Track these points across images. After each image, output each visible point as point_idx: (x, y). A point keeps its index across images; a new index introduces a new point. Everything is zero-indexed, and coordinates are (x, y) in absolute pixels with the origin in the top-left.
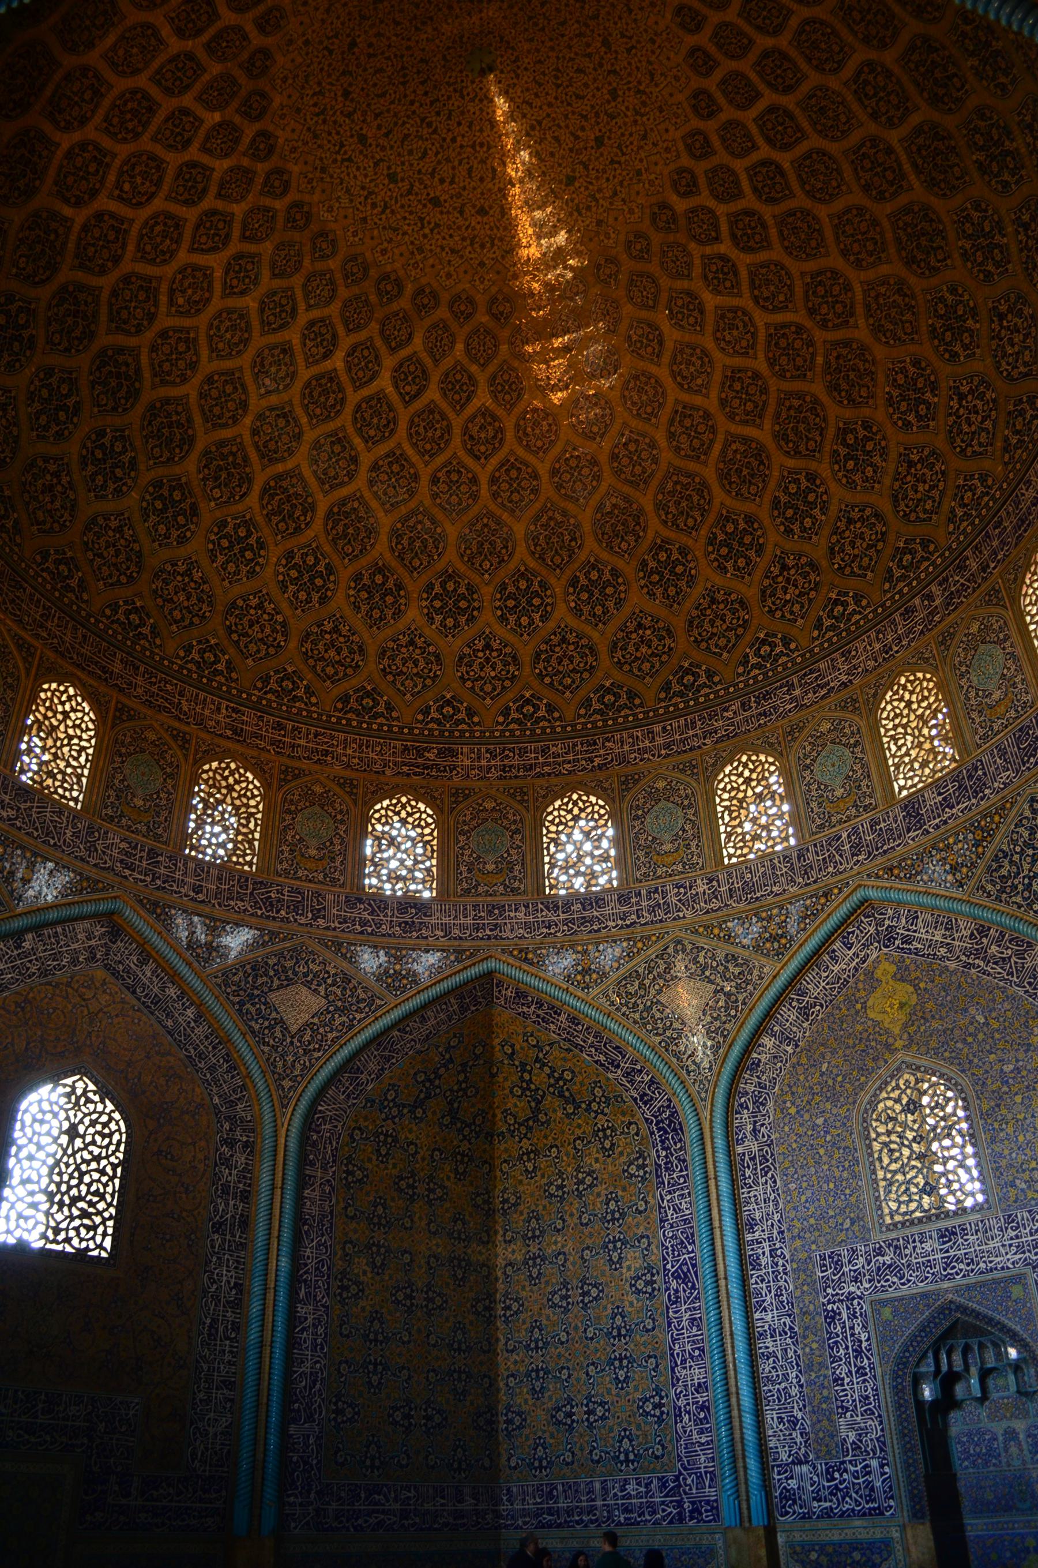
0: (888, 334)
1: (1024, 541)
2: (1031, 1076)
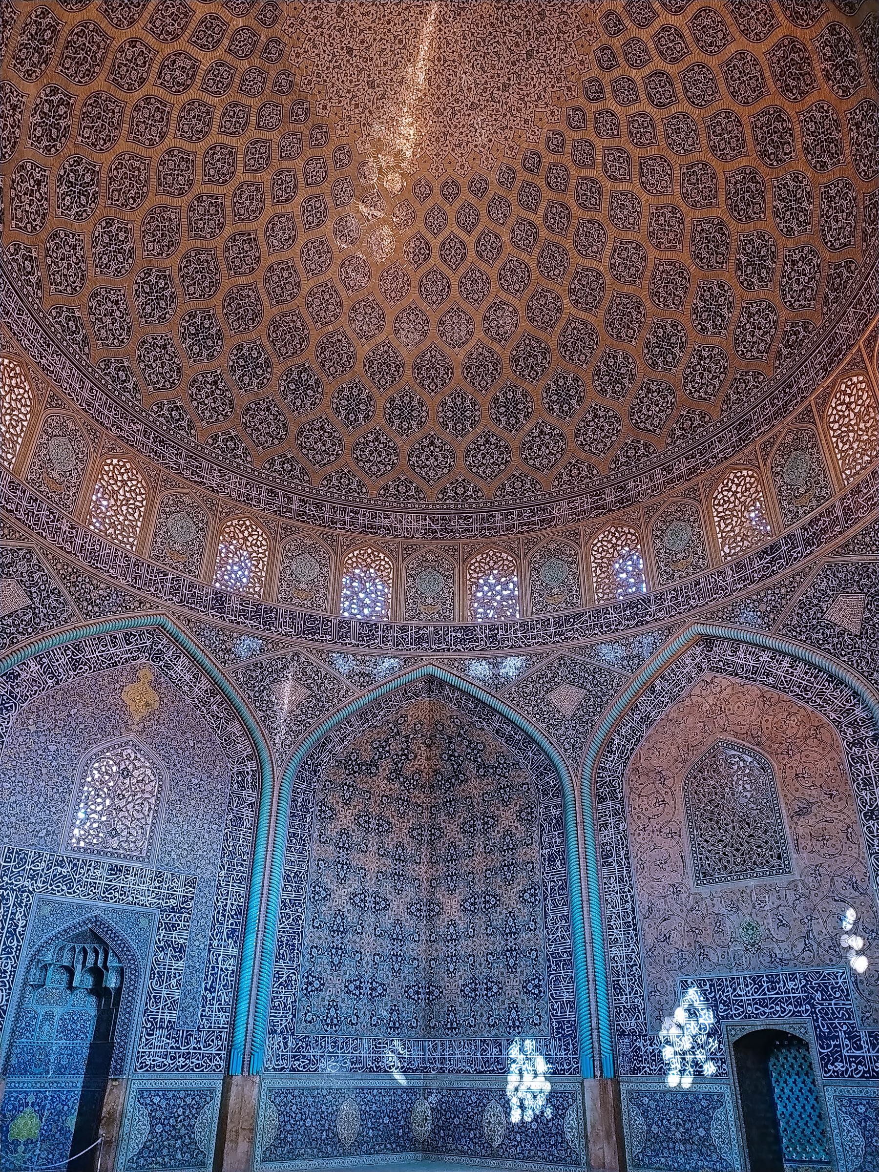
0: (371, 370)
2: (205, 793)
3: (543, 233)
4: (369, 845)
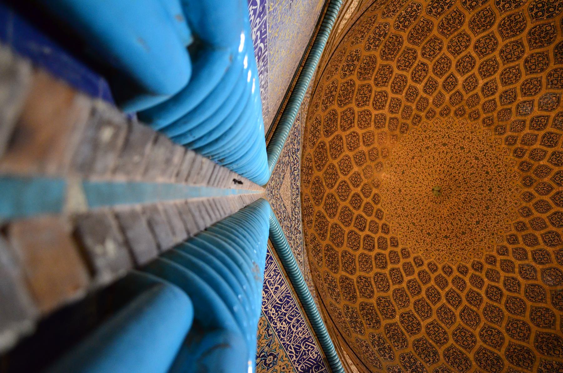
3: (404, 285)
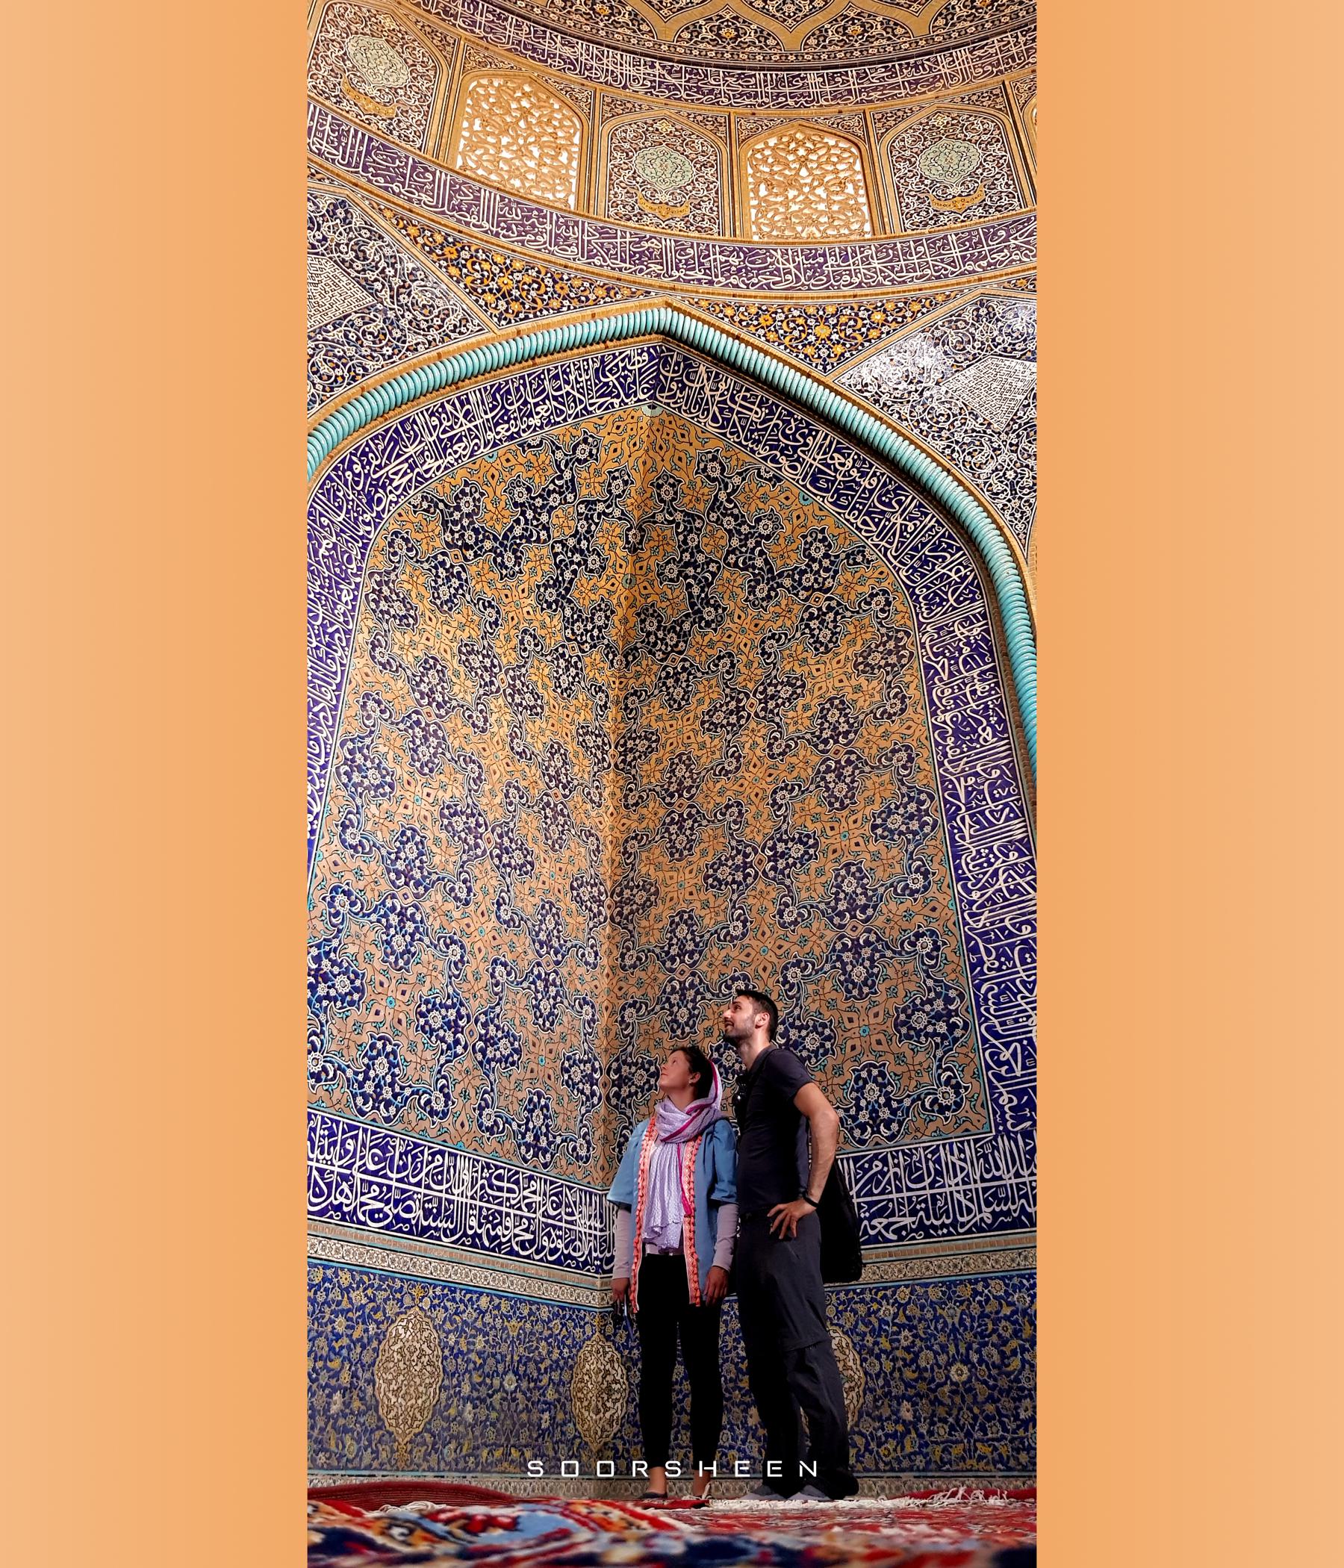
1: (524, 60)
4: (492, 720)
